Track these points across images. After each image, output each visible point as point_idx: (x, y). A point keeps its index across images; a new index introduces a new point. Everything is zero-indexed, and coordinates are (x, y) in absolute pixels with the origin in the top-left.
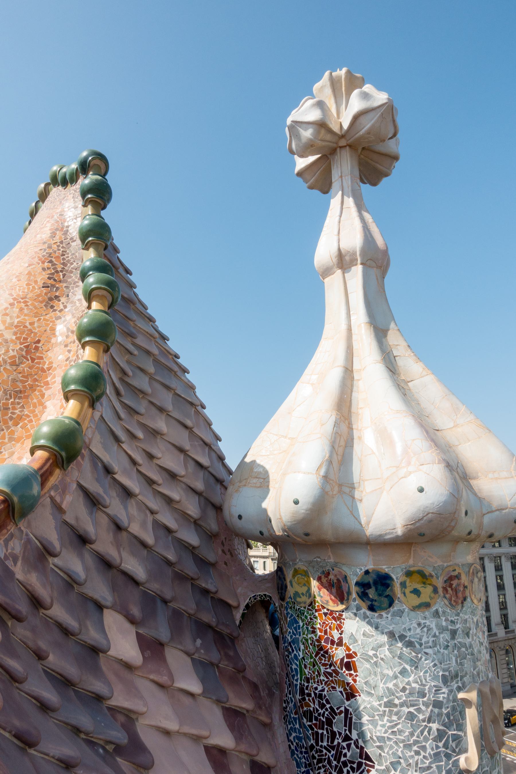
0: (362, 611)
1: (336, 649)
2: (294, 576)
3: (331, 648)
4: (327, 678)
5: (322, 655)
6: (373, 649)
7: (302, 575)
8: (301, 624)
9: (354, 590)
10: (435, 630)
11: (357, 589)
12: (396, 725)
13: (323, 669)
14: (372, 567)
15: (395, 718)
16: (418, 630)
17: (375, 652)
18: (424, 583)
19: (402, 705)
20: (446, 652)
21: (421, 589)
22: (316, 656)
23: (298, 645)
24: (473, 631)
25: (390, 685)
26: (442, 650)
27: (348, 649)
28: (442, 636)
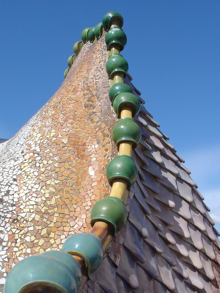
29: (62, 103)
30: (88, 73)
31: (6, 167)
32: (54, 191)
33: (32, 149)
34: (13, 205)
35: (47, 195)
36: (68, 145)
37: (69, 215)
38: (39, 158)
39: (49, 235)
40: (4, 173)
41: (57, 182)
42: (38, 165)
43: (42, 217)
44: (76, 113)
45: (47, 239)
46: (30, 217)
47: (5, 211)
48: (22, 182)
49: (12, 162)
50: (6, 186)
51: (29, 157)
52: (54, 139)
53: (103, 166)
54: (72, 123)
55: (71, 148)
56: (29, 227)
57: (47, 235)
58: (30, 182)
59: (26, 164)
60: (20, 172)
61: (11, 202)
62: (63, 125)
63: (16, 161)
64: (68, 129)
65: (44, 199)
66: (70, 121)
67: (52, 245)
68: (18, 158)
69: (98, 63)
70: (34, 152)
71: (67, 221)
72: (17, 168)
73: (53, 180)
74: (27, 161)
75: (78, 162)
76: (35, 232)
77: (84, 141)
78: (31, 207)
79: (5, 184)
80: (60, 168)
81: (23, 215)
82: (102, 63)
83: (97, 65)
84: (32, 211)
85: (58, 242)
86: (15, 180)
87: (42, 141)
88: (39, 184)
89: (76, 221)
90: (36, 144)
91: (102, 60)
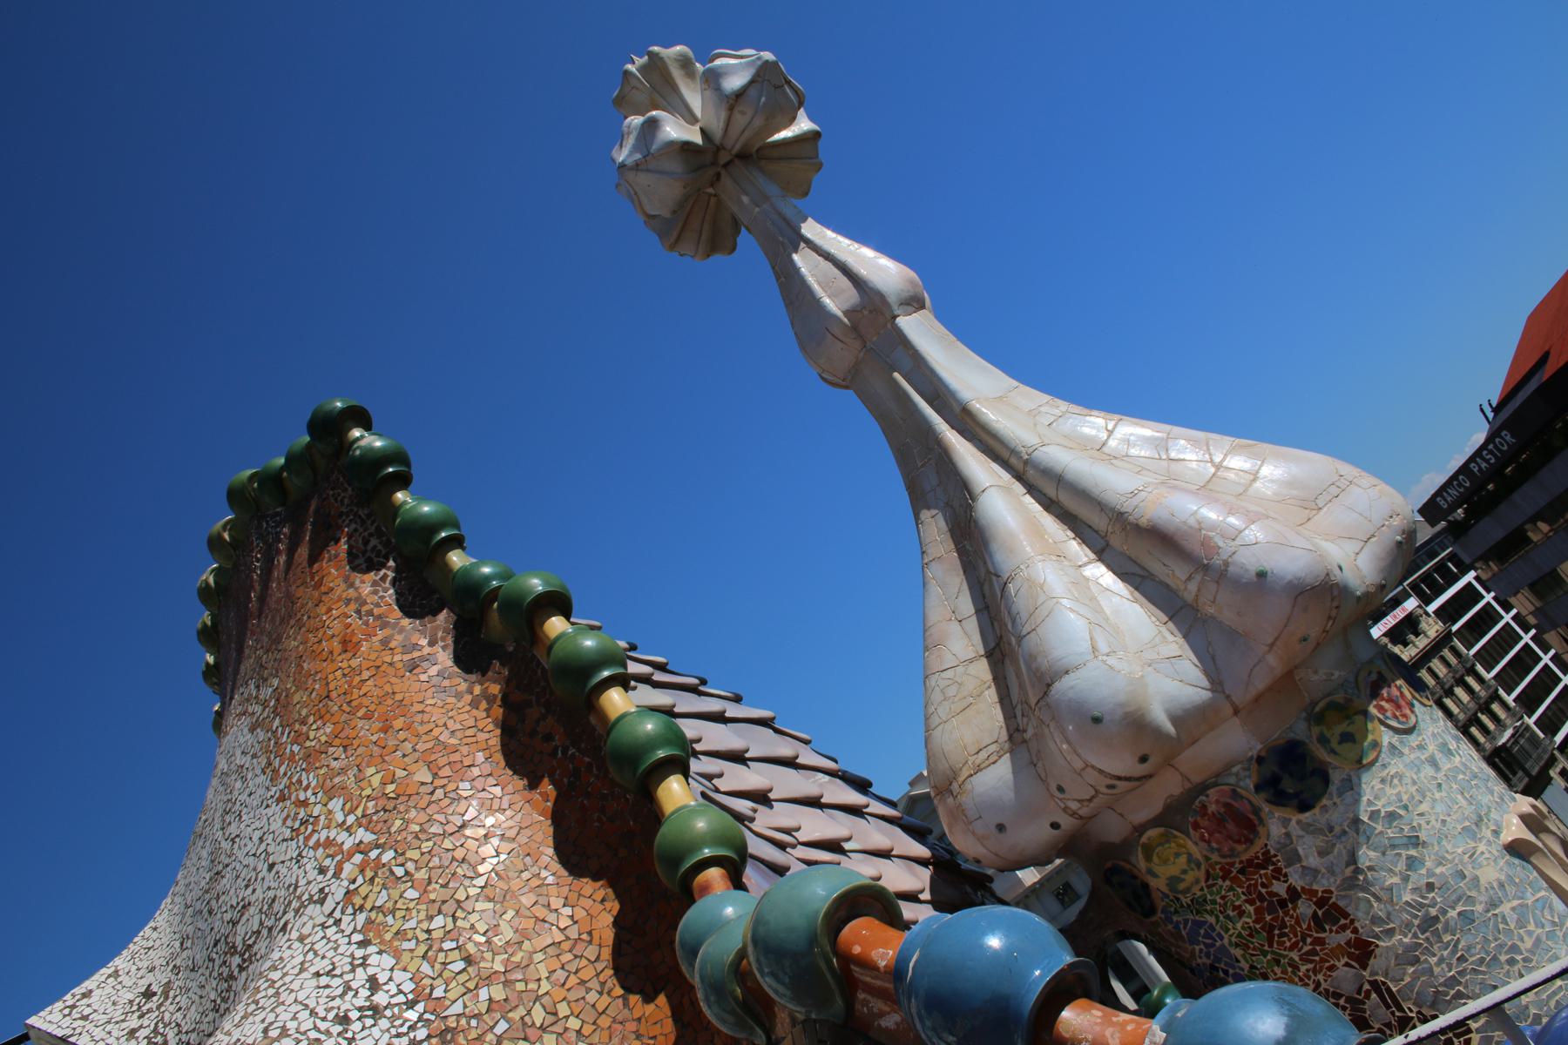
0: (1293, 822)
1: (1294, 909)
2: (1148, 858)
3: (1286, 914)
4: (1311, 961)
5: (1280, 936)
6: (1347, 865)
7: (1161, 844)
8: (1212, 920)
9: (1259, 800)
10: (1410, 774)
11: (1263, 795)
12: (1455, 946)
13: (1295, 955)
14: (1259, 746)
15: (1447, 938)
16: (1389, 791)
17: (1352, 868)
18: (1348, 717)
19: (1444, 912)
20: (1444, 794)
21: (1350, 729)
22: (1271, 945)
23: (1229, 955)
24: (1453, 745)
25: (1407, 897)
26: (1437, 795)
27: (1313, 893)
28: (1422, 775)
29: (334, 695)
30: (352, 585)
31: (305, 931)
33: (346, 847)
34: (411, 1005)
35: (482, 927)
36: (438, 782)
37: (568, 938)
38: (391, 853)
39: (555, 1014)
40: (316, 947)
41: (481, 882)
42: (399, 872)
43: (507, 983)
44: (398, 697)
45: (558, 1028)
47: (404, 1029)
48: (388, 936)
49: (313, 910)
50: (353, 971)
51: (357, 871)
52: (390, 788)
54: (408, 727)
55: (451, 786)
56: (492, 1028)
57: (551, 1019)
58: (412, 924)
59: (364, 890)
60: (361, 918)
61: (401, 998)
63: (322, 902)
64: (408, 746)
65: (483, 939)
66: (398, 723)
67: (578, 1032)
68: (321, 890)
70: (360, 848)
72: (343, 913)
73: (467, 882)
74: (360, 880)
75: (496, 807)
78: (463, 978)
79: (348, 967)
81: (457, 1008)
82: (374, 542)
83: (364, 553)
84: (471, 985)
85: (589, 1016)
86: (363, 944)
87: (359, 812)
88: (440, 912)
90: (348, 829)
91: (371, 535)
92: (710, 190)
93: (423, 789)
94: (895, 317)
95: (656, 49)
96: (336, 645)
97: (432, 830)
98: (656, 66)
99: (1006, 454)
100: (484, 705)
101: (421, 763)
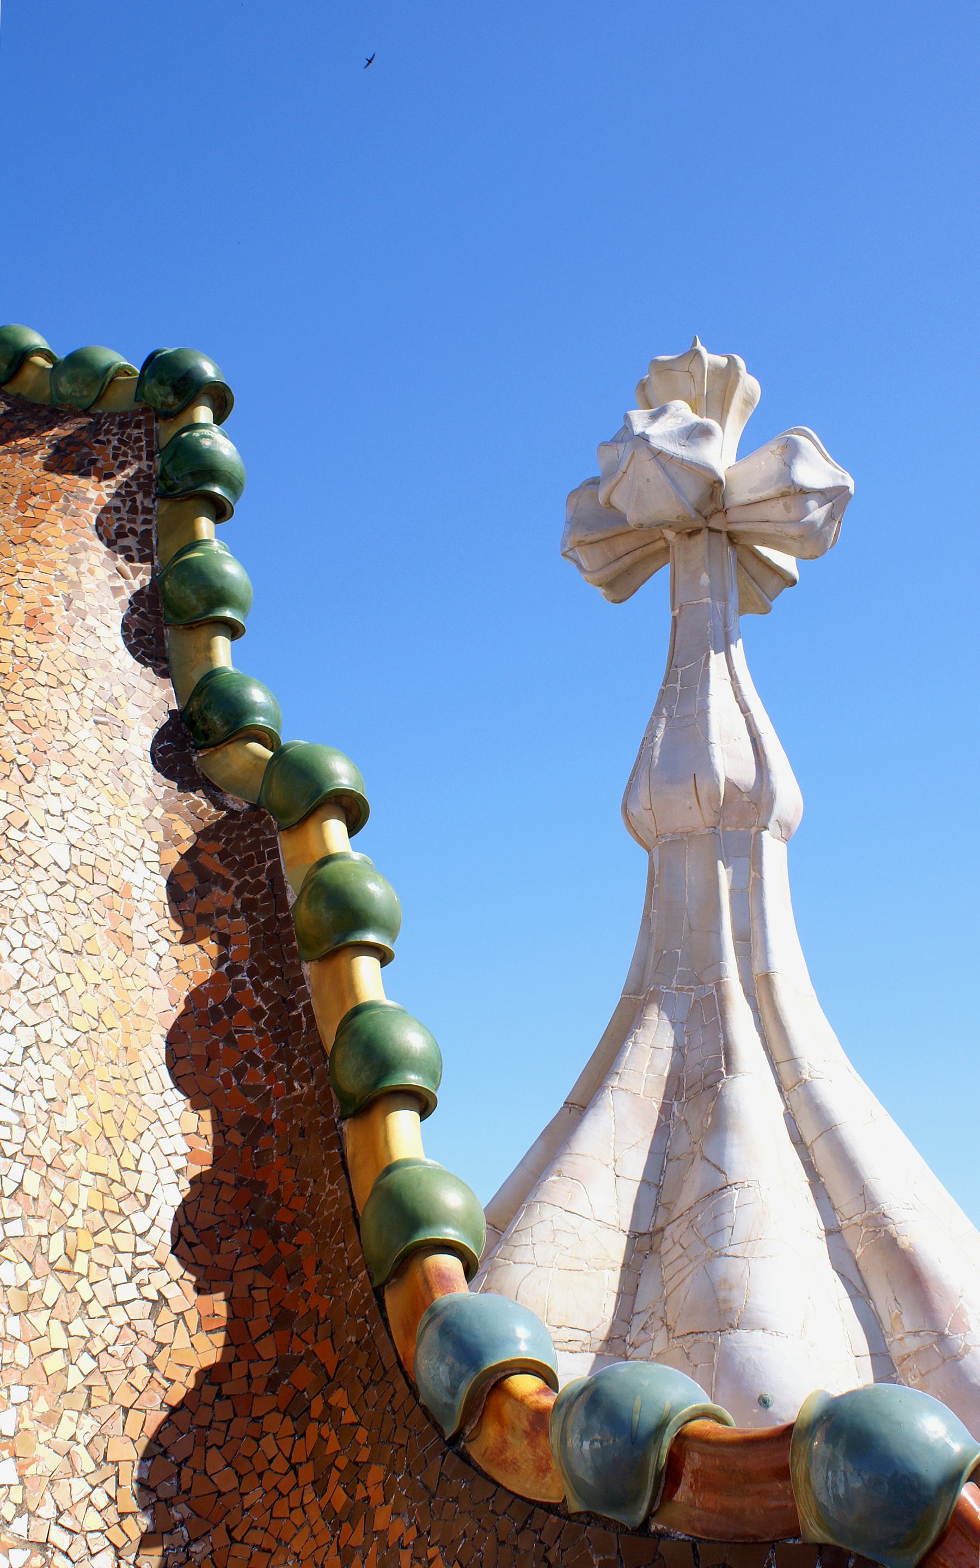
30: (77, 564)
32: (69, 1073)
36: (71, 876)
37: (123, 1183)
39: (72, 1261)
44: (69, 737)
46: (6, 1176)
53: (211, 1003)
57: (63, 1263)
62: (33, 780)
67: (85, 1304)
69: (114, 537)
71: (120, 1209)
76: (29, 1246)
77: (126, 875)
80: (68, 974)
89: (151, 1211)
91: (133, 531)
92: (670, 535)
93: (53, 869)
94: (766, 828)
95: (741, 362)
96: (19, 609)
97: (47, 928)
98: (728, 376)
99: (779, 1056)
100: (159, 836)
101: (61, 838)
